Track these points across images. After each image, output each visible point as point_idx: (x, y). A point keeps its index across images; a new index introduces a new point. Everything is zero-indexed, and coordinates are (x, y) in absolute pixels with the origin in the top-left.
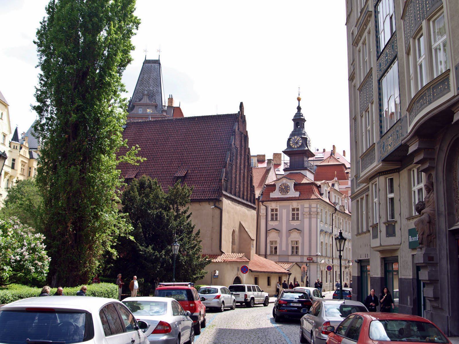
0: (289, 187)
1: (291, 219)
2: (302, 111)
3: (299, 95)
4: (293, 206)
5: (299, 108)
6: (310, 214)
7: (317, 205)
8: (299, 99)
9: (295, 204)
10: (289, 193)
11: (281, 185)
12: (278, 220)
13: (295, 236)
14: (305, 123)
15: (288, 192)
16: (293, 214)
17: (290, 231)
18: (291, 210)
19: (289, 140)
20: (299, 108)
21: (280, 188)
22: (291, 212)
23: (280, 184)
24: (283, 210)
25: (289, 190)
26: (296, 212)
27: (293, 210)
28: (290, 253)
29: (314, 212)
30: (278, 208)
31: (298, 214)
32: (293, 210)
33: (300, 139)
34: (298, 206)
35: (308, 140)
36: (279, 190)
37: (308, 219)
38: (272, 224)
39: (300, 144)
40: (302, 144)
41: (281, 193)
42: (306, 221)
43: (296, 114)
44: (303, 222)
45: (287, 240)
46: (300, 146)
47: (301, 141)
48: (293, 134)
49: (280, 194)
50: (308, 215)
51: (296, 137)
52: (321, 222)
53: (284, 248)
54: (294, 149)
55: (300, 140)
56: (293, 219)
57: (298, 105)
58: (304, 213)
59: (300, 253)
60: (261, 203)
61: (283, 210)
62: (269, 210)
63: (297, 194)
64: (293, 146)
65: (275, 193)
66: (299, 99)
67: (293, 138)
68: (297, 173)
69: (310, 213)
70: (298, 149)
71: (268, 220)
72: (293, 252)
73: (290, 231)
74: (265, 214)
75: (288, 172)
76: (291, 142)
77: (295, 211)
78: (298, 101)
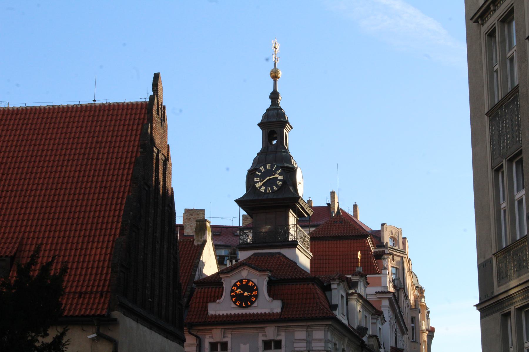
5: (275, 96)
8: (275, 76)
10: (255, 304)
11: (235, 285)
15: (253, 303)
20: (275, 96)
21: (232, 291)
23: (233, 282)
36: (232, 297)
41: (235, 303)
49: (233, 305)
57: (272, 90)
63: (276, 307)
65: (219, 303)
66: (275, 76)
78: (272, 81)
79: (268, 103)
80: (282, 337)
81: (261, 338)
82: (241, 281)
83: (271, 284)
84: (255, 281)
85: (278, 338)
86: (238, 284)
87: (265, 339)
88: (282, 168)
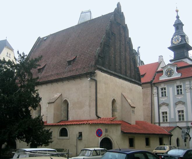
0: (173, 70)
1: (176, 94)
2: (180, 19)
4: (176, 84)
5: (178, 17)
8: (177, 11)
9: (178, 83)
10: (173, 75)
11: (166, 70)
12: (167, 96)
13: (180, 107)
14: (183, 27)
15: (172, 75)
16: (178, 91)
17: (176, 104)
18: (175, 87)
19: (172, 39)
20: (178, 17)
21: (166, 72)
22: (176, 89)
23: (166, 70)
24: (170, 88)
25: (173, 73)
26: (179, 88)
28: (177, 120)
31: (181, 90)
32: (178, 87)
33: (180, 37)
35: (186, 37)
36: (166, 74)
38: (163, 100)
39: (180, 40)
40: (182, 40)
41: (167, 76)
43: (176, 21)
44: (185, 95)
46: (180, 42)
47: (181, 38)
48: (174, 35)
49: (166, 77)
51: (176, 36)
53: (172, 117)
54: (176, 45)
55: (180, 38)
56: (178, 94)
59: (185, 120)
60: (153, 85)
61: (170, 88)
62: (160, 89)
64: (175, 43)
66: (177, 11)
67: (175, 37)
68: (180, 61)
69: (190, 88)
70: (179, 44)
72: (180, 119)
73: (176, 104)
75: (173, 62)
76: (173, 41)
78: (176, 13)
79: (176, 19)
80: (182, 84)
81: (175, 85)
82: (168, 69)
83: (177, 69)
84: (172, 68)
85: (181, 84)
86: (168, 70)
87: (177, 85)
88: (180, 36)
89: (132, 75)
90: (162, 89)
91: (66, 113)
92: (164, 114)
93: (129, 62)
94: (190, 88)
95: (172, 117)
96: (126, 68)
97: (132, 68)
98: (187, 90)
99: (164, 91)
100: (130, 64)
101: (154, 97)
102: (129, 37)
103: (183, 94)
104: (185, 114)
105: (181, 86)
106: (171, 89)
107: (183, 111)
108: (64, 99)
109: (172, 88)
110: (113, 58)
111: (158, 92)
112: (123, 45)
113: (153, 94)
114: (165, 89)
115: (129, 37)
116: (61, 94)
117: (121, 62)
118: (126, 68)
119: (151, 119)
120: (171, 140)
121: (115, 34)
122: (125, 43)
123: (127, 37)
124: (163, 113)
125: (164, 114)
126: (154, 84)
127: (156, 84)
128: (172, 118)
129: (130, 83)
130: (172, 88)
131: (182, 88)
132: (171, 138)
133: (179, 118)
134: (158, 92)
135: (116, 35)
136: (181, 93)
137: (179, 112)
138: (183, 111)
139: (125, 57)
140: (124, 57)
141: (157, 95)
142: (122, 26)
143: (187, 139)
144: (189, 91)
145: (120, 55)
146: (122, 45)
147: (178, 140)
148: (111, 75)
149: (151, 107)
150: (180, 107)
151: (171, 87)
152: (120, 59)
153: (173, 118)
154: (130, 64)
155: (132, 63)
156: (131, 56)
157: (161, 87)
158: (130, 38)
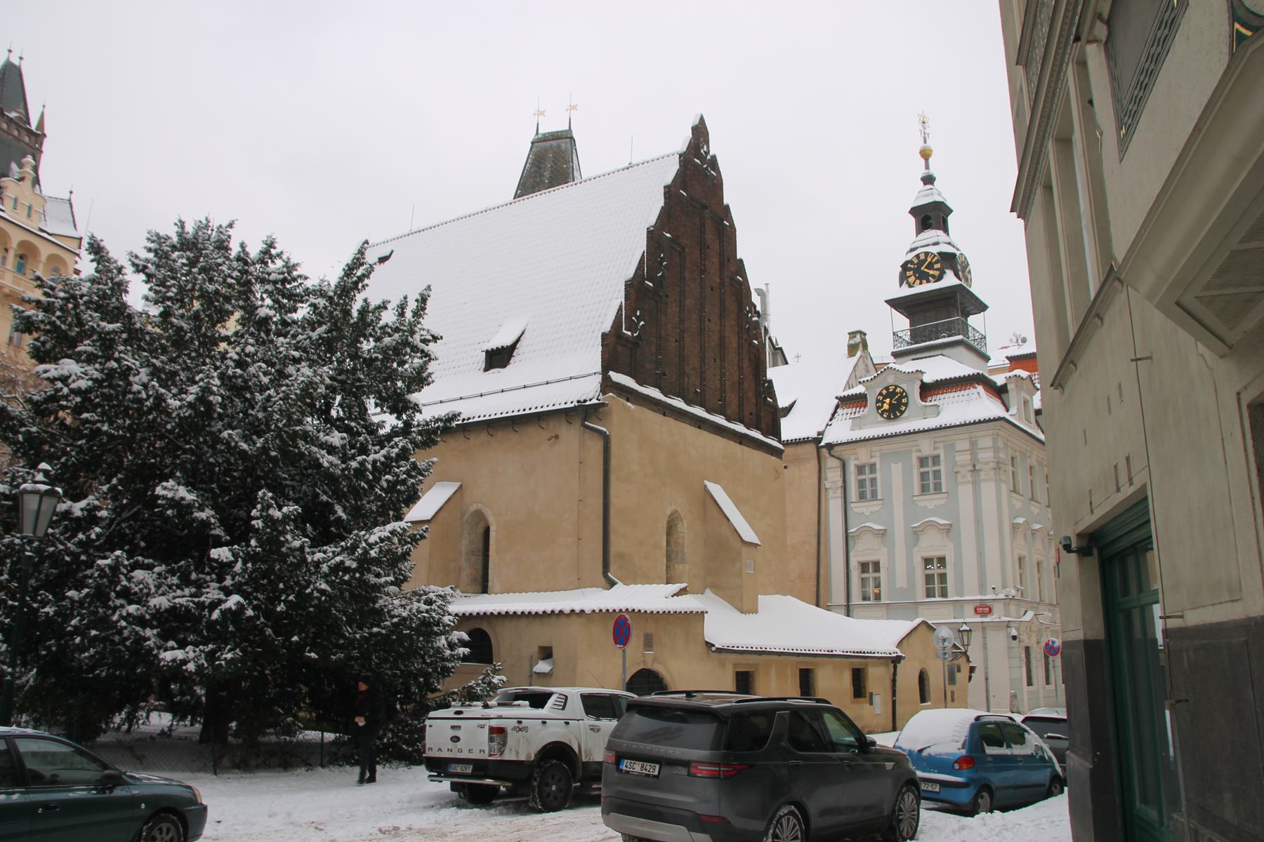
0: (906, 396)
1: (917, 489)
3: (925, 142)
4: (920, 451)
6: (974, 470)
7: (995, 440)
8: (926, 154)
10: (905, 415)
11: (881, 394)
15: (902, 413)
16: (923, 476)
18: (915, 461)
21: (878, 401)
24: (893, 465)
25: (906, 405)
26: (930, 469)
27: (923, 461)
29: (986, 463)
30: (877, 460)
31: (937, 474)
32: (923, 461)
34: (935, 449)
36: (878, 408)
37: (970, 487)
41: (881, 415)
42: (965, 492)
45: (909, 556)
49: (880, 418)
50: (969, 475)
52: (1014, 495)
56: (924, 489)
58: (955, 470)
60: (825, 451)
61: (893, 465)
62: (852, 469)
66: (926, 154)
69: (974, 466)
71: (848, 501)
74: (840, 483)
77: (927, 466)
78: (923, 161)
81: (914, 457)
82: (887, 389)
84: (904, 386)
86: (884, 392)
89: (747, 413)
90: (860, 470)
91: (480, 566)
92: (868, 572)
93: (736, 360)
94: (974, 466)
95: (901, 582)
96: (722, 385)
97: (748, 385)
98: (959, 476)
99: (867, 476)
100: (739, 366)
101: (827, 500)
102: (738, 257)
103: (944, 490)
104: (949, 571)
105: (936, 459)
106: (897, 469)
107: (942, 561)
108: (473, 508)
109: (900, 465)
110: (672, 345)
111: (844, 481)
112: (712, 289)
113: (826, 489)
114: (873, 467)
115: (738, 257)
116: (461, 485)
117: (703, 360)
118: (722, 385)
119: (814, 589)
120: (897, 678)
121: (684, 248)
122: (722, 284)
123: (729, 260)
124: (864, 567)
125: (868, 572)
126: (830, 446)
127: (836, 449)
128: (898, 586)
129: (737, 445)
130: (900, 465)
131: (942, 468)
132: (895, 668)
133: (927, 588)
134: (844, 481)
135: (687, 250)
136: (938, 488)
137: (928, 561)
138: (942, 561)
139: (722, 338)
140: (716, 338)
141: (839, 493)
142: (711, 212)
143: (959, 670)
144: (969, 479)
145: (702, 331)
146: (708, 290)
147: (922, 679)
148: (664, 415)
149: (814, 541)
150: (932, 545)
151: (896, 463)
152: (702, 348)
153: (905, 587)
154: (740, 369)
155: (746, 364)
156: (745, 337)
157: (857, 462)
158: (741, 261)
